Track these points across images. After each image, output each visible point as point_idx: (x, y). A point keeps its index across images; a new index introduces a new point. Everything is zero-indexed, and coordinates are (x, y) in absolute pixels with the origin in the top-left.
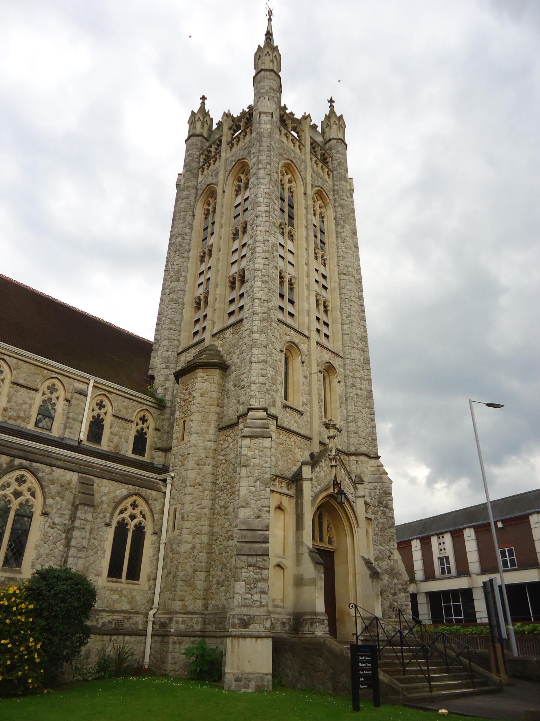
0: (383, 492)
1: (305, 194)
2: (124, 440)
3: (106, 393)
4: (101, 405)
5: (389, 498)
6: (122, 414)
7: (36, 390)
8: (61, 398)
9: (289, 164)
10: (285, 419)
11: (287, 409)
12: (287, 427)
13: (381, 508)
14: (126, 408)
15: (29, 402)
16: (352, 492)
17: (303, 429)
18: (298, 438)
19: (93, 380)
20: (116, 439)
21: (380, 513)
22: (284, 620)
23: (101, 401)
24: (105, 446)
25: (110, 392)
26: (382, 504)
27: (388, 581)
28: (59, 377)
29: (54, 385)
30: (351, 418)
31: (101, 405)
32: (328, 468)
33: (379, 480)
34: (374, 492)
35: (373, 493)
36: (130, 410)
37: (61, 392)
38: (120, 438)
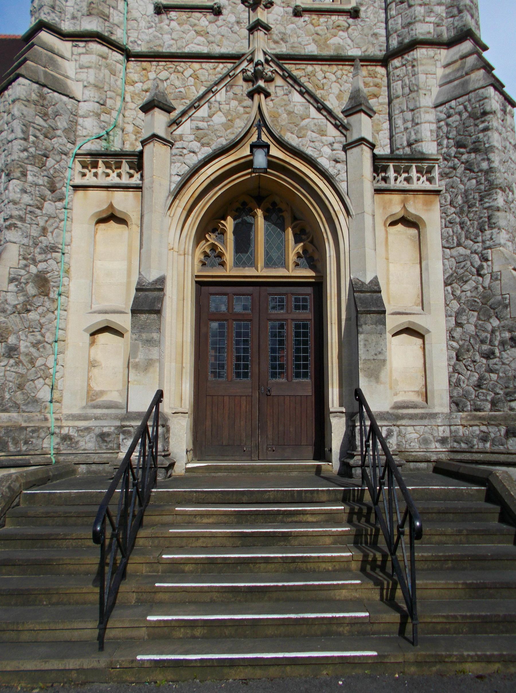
0: (470, 116)
5: (481, 126)
10: (166, 37)
11: (173, 14)
13: (465, 157)
16: (331, 140)
17: (225, 42)
18: (204, 65)
21: (461, 169)
22: (105, 430)
26: (464, 146)
27: (476, 326)
32: (240, 101)
33: (456, 93)
34: (448, 125)
35: (445, 129)
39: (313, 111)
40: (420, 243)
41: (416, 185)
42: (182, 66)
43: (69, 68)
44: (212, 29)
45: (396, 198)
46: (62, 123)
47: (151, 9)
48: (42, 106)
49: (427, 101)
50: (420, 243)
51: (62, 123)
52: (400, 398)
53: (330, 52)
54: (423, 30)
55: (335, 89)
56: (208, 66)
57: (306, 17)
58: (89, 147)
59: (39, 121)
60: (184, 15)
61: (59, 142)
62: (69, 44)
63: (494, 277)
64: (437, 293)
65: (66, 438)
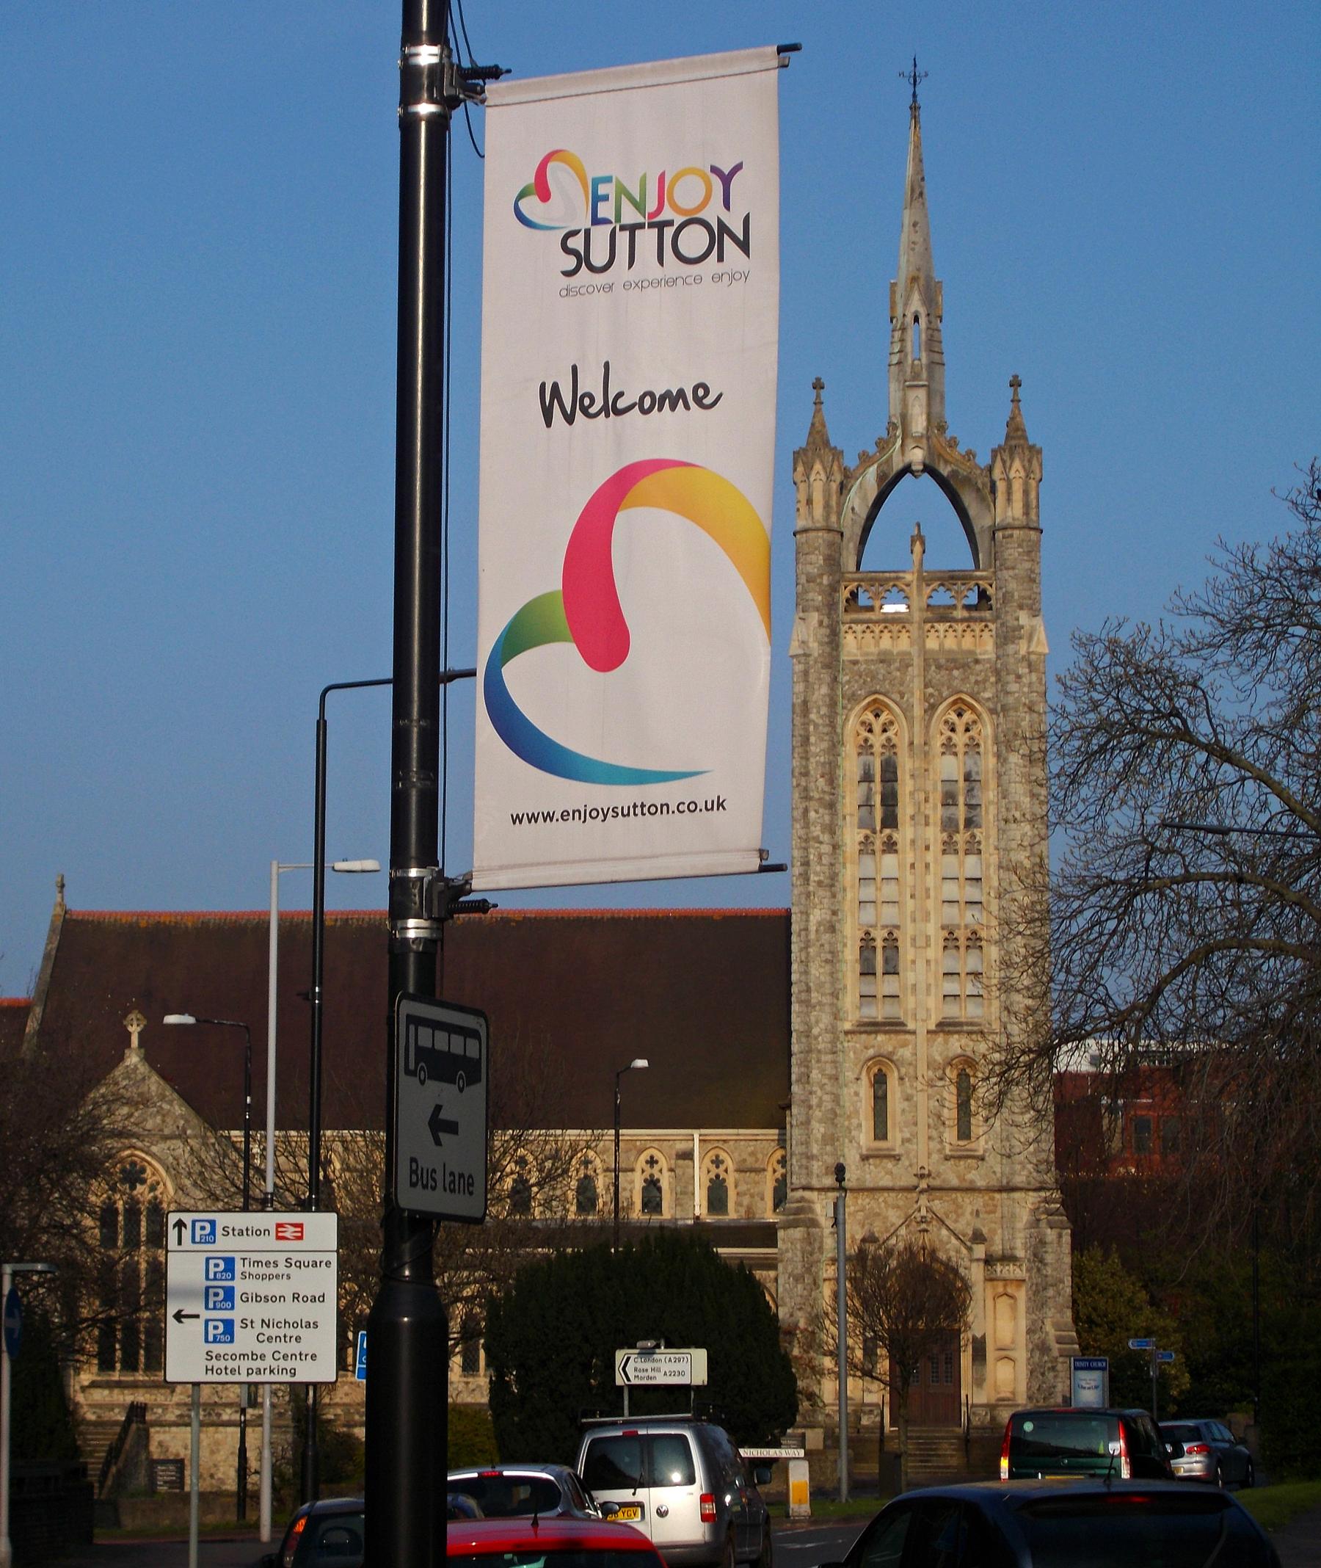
1: (911, 743)
2: (757, 1198)
3: (720, 1144)
4: (717, 1162)
6: (750, 1162)
7: (632, 1170)
8: (665, 1170)
9: (875, 701)
11: (871, 1161)
12: (871, 1185)
14: (753, 1154)
15: (629, 1187)
19: (696, 1134)
20: (746, 1201)
23: (717, 1156)
24: (733, 1214)
25: (725, 1141)
28: (655, 1144)
29: (652, 1157)
30: (1004, 1135)
31: (717, 1162)
36: (760, 1156)
37: (663, 1163)
38: (752, 1196)
39: (954, 1241)
40: (1014, 1308)
41: (1012, 1276)
42: (877, 1195)
43: (818, 1208)
44: (895, 1170)
45: (1001, 1284)
46: (817, 1245)
47: (858, 1157)
48: (809, 1239)
49: (1020, 1225)
50: (1014, 1308)
51: (817, 1245)
52: (1002, 1395)
53: (966, 1185)
54: (1019, 1180)
55: (969, 1209)
56: (893, 1194)
57: (952, 1161)
58: (830, 1255)
59: (808, 1248)
60: (878, 1161)
61: (816, 1256)
62: (816, 1193)
63: (1047, 1333)
64: (1022, 1338)
65: (828, 1415)
